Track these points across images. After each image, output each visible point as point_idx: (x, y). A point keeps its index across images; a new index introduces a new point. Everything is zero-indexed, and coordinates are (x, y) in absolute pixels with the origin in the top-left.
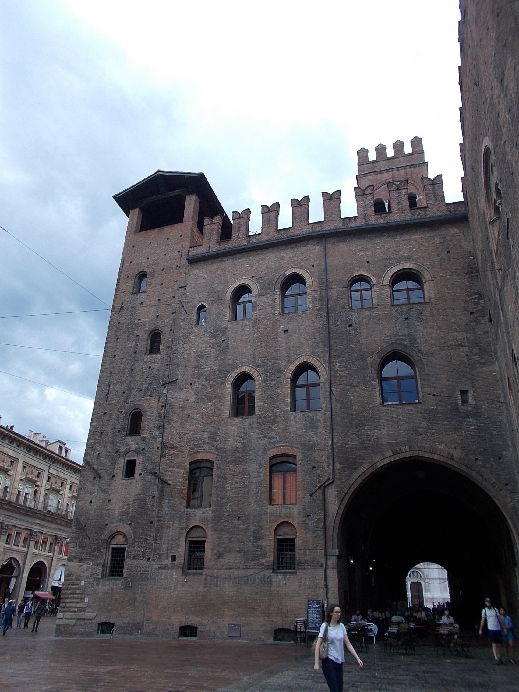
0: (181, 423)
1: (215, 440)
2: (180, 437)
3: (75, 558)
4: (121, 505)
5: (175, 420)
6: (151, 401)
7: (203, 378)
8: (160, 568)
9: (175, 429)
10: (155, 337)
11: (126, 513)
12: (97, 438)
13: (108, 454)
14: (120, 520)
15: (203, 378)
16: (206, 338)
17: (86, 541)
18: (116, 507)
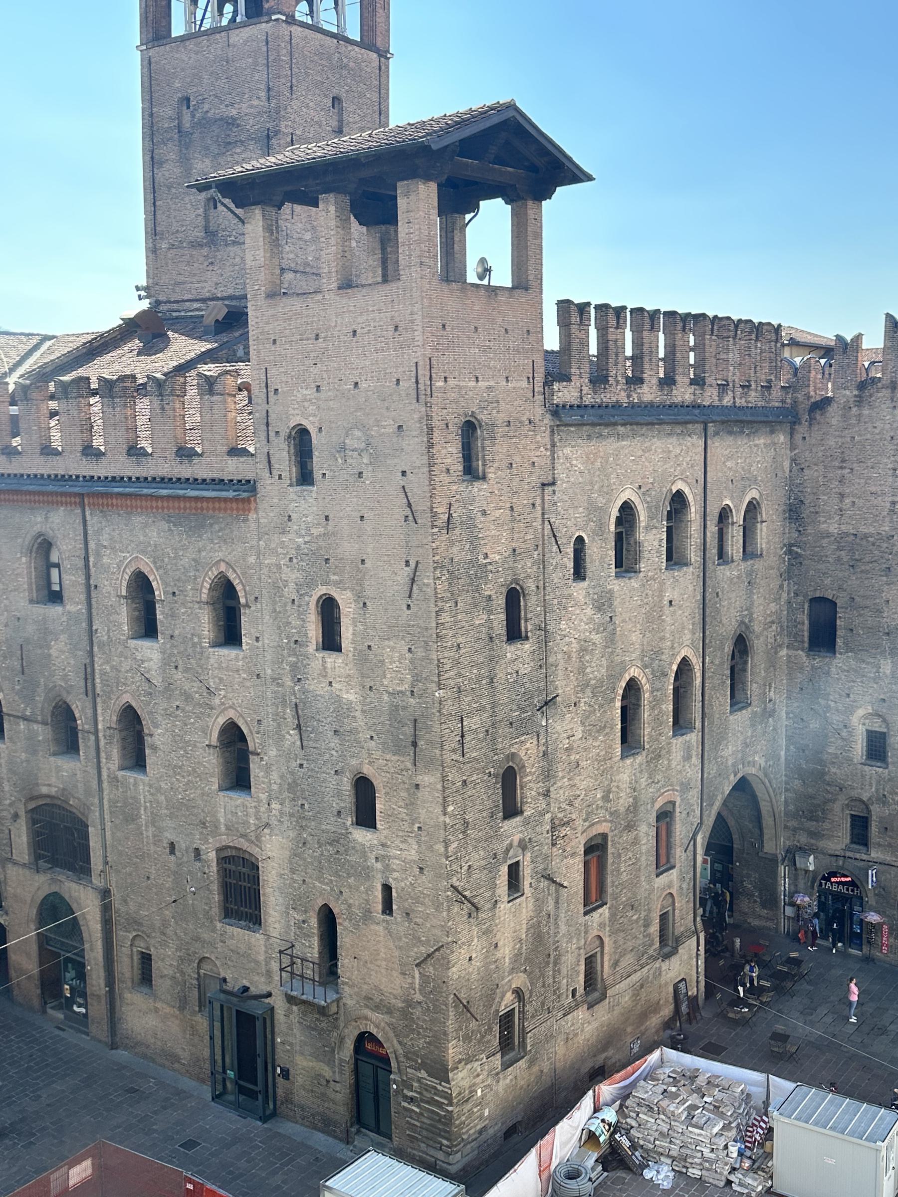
0: (569, 779)
1: (609, 801)
2: (571, 804)
3: (460, 1061)
4: (512, 945)
5: (560, 774)
6: (528, 745)
7: (588, 692)
8: (565, 1015)
9: (561, 792)
10: (513, 599)
11: (518, 955)
12: (461, 836)
13: (483, 863)
14: (512, 970)
15: (588, 692)
16: (589, 611)
17: (473, 1024)
18: (506, 952)
